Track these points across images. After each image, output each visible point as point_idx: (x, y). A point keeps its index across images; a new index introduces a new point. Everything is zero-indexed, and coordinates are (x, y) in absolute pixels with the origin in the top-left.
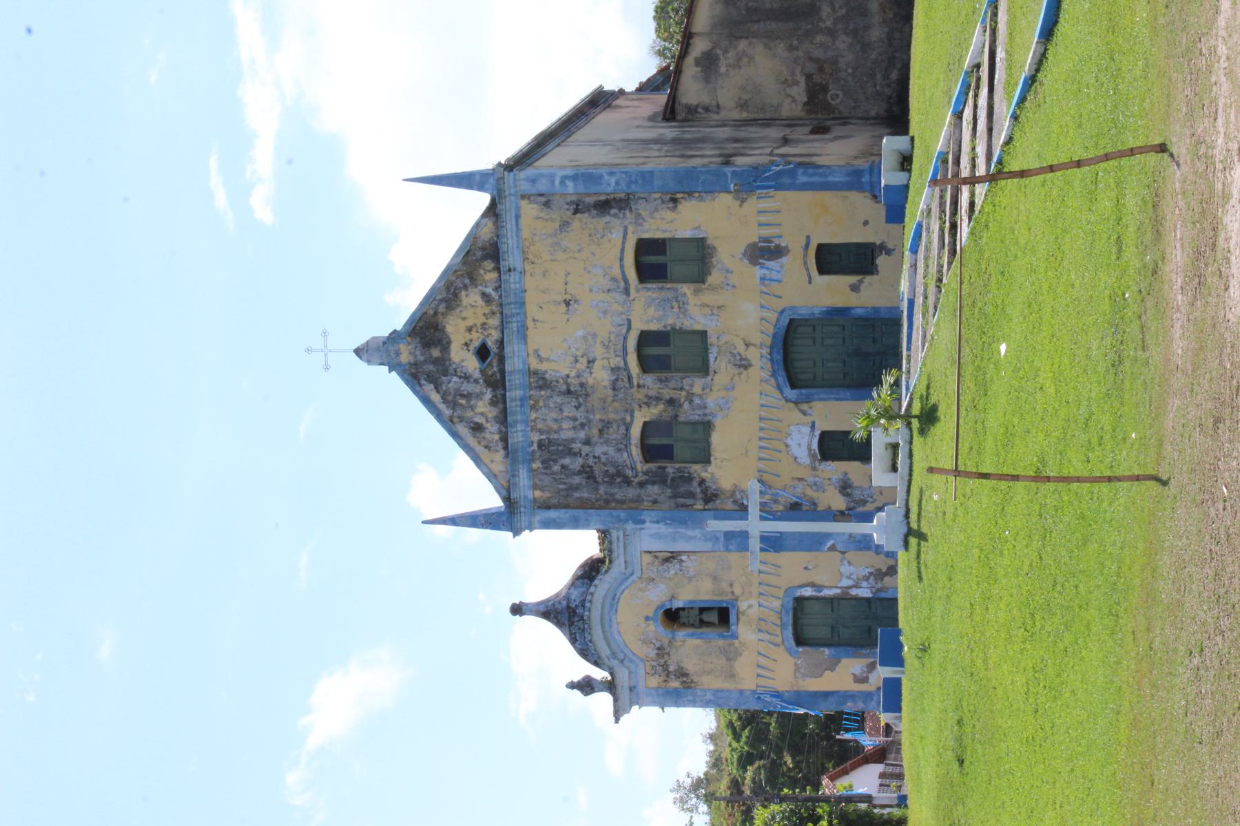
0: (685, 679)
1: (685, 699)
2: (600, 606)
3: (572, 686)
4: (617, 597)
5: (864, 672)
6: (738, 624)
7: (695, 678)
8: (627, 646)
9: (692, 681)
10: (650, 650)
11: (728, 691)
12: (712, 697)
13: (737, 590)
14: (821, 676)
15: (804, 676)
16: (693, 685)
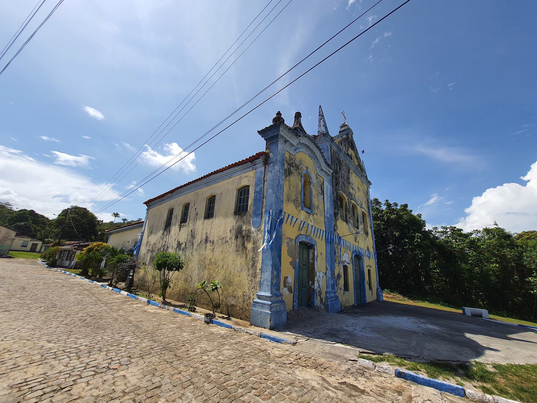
0: (288, 173)
1: (281, 167)
2: (314, 150)
3: (279, 114)
4: (313, 159)
5: (288, 285)
6: (306, 212)
7: (288, 178)
8: (299, 152)
9: (287, 176)
10: (298, 162)
11: (283, 194)
12: (281, 183)
13: (315, 215)
14: (288, 254)
15: (288, 243)
16: (285, 176)
